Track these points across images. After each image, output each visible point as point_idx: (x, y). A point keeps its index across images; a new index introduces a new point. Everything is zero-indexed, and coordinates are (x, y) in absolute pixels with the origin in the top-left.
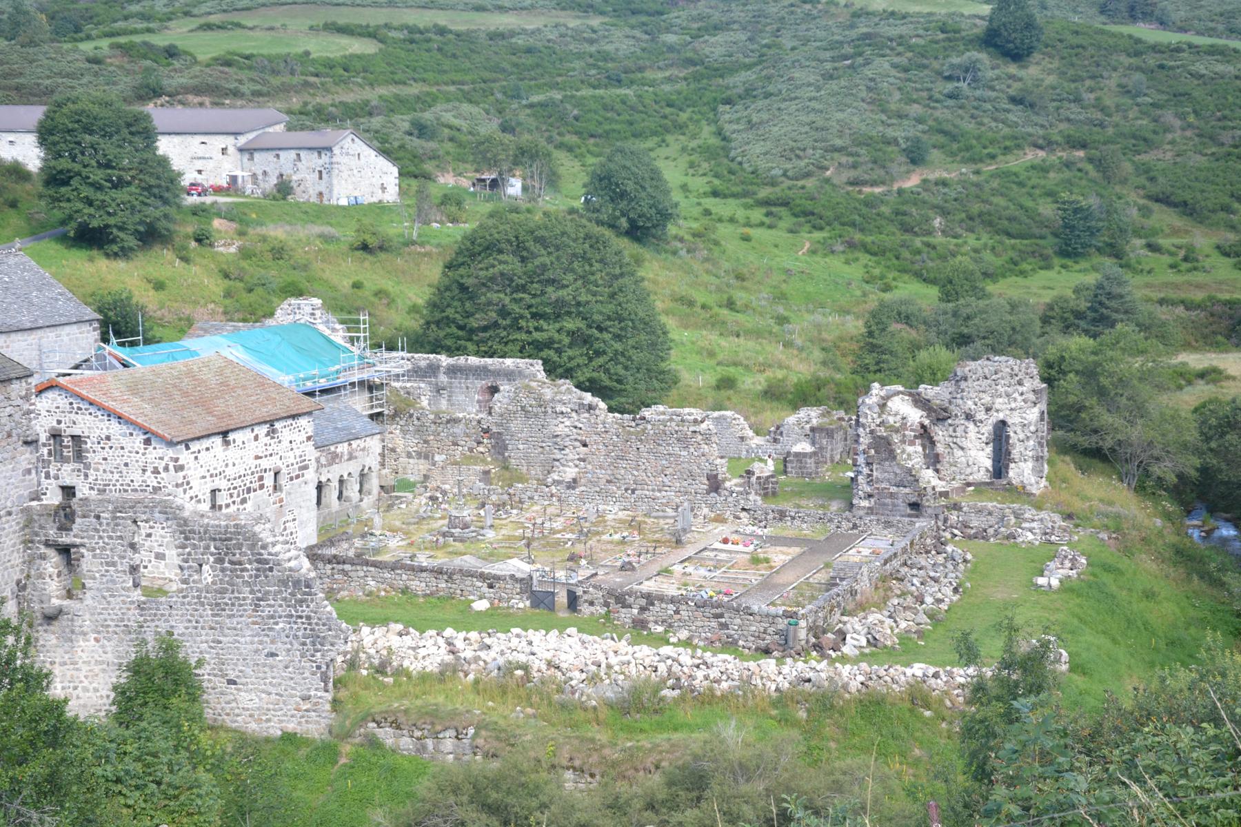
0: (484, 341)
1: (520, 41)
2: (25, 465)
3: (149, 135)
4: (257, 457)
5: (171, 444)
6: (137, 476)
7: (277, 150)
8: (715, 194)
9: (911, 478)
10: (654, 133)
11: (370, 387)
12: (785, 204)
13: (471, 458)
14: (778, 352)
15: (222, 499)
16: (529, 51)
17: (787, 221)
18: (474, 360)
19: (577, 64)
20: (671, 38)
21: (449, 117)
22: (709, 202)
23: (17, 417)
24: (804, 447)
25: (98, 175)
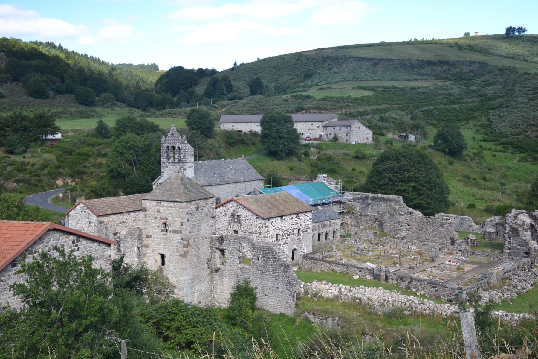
0: (384, 189)
1: (421, 90)
2: (211, 224)
3: (291, 123)
5: (264, 219)
6: (254, 228)
7: (334, 126)
8: (485, 140)
9: (525, 243)
10: (465, 120)
11: (340, 203)
12: (510, 144)
13: (371, 228)
14: (499, 195)
15: (280, 237)
16: (424, 93)
17: (511, 150)
18: (380, 195)
19: (440, 97)
20: (474, 88)
21: (393, 115)
22: (483, 144)
23: (209, 209)
24: (492, 230)
25: (275, 135)
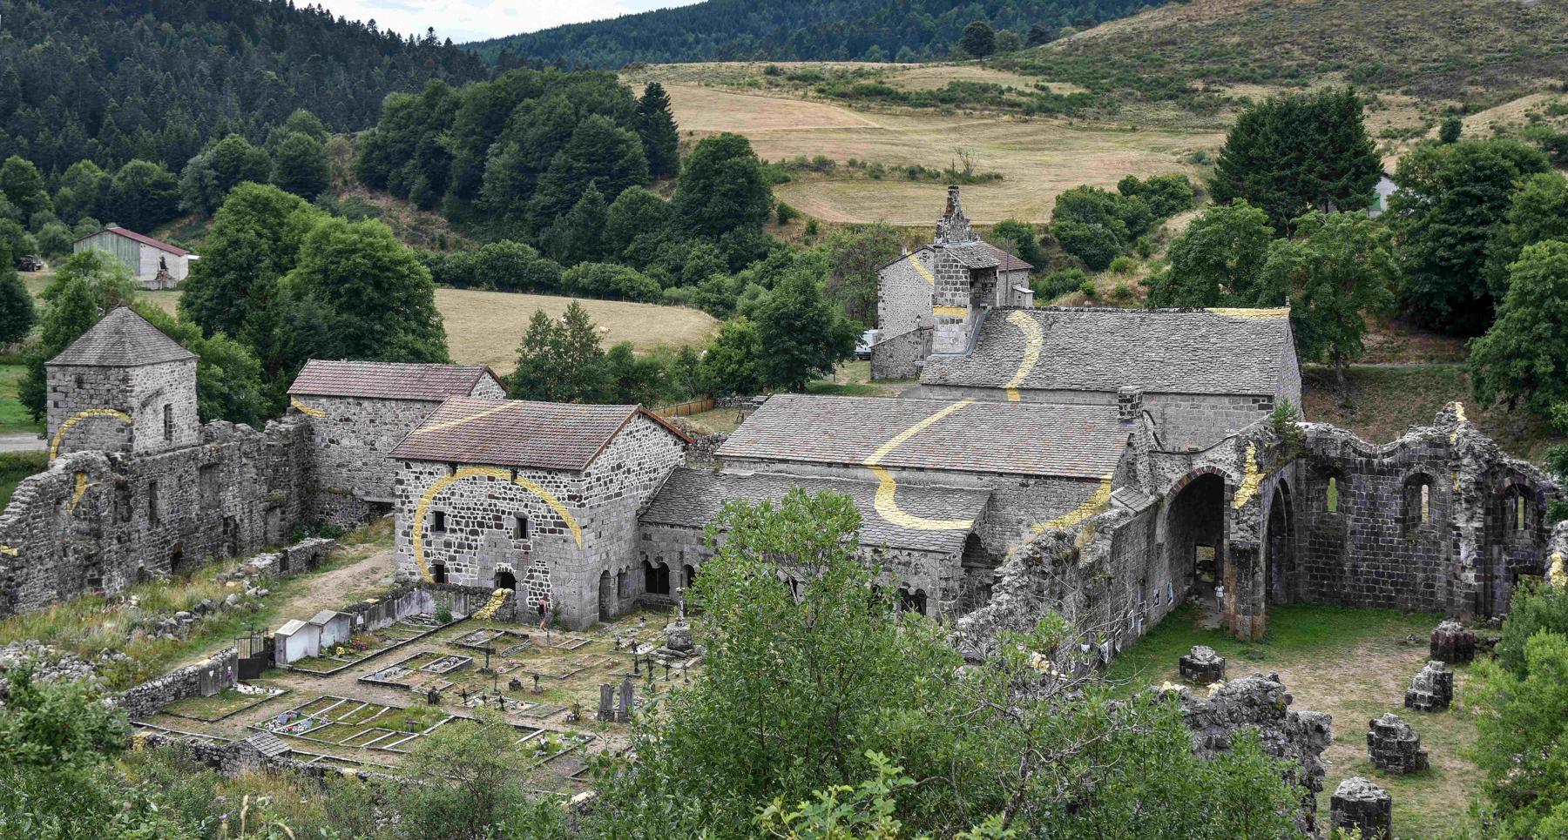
4: (491, 497)
15: (449, 523)
